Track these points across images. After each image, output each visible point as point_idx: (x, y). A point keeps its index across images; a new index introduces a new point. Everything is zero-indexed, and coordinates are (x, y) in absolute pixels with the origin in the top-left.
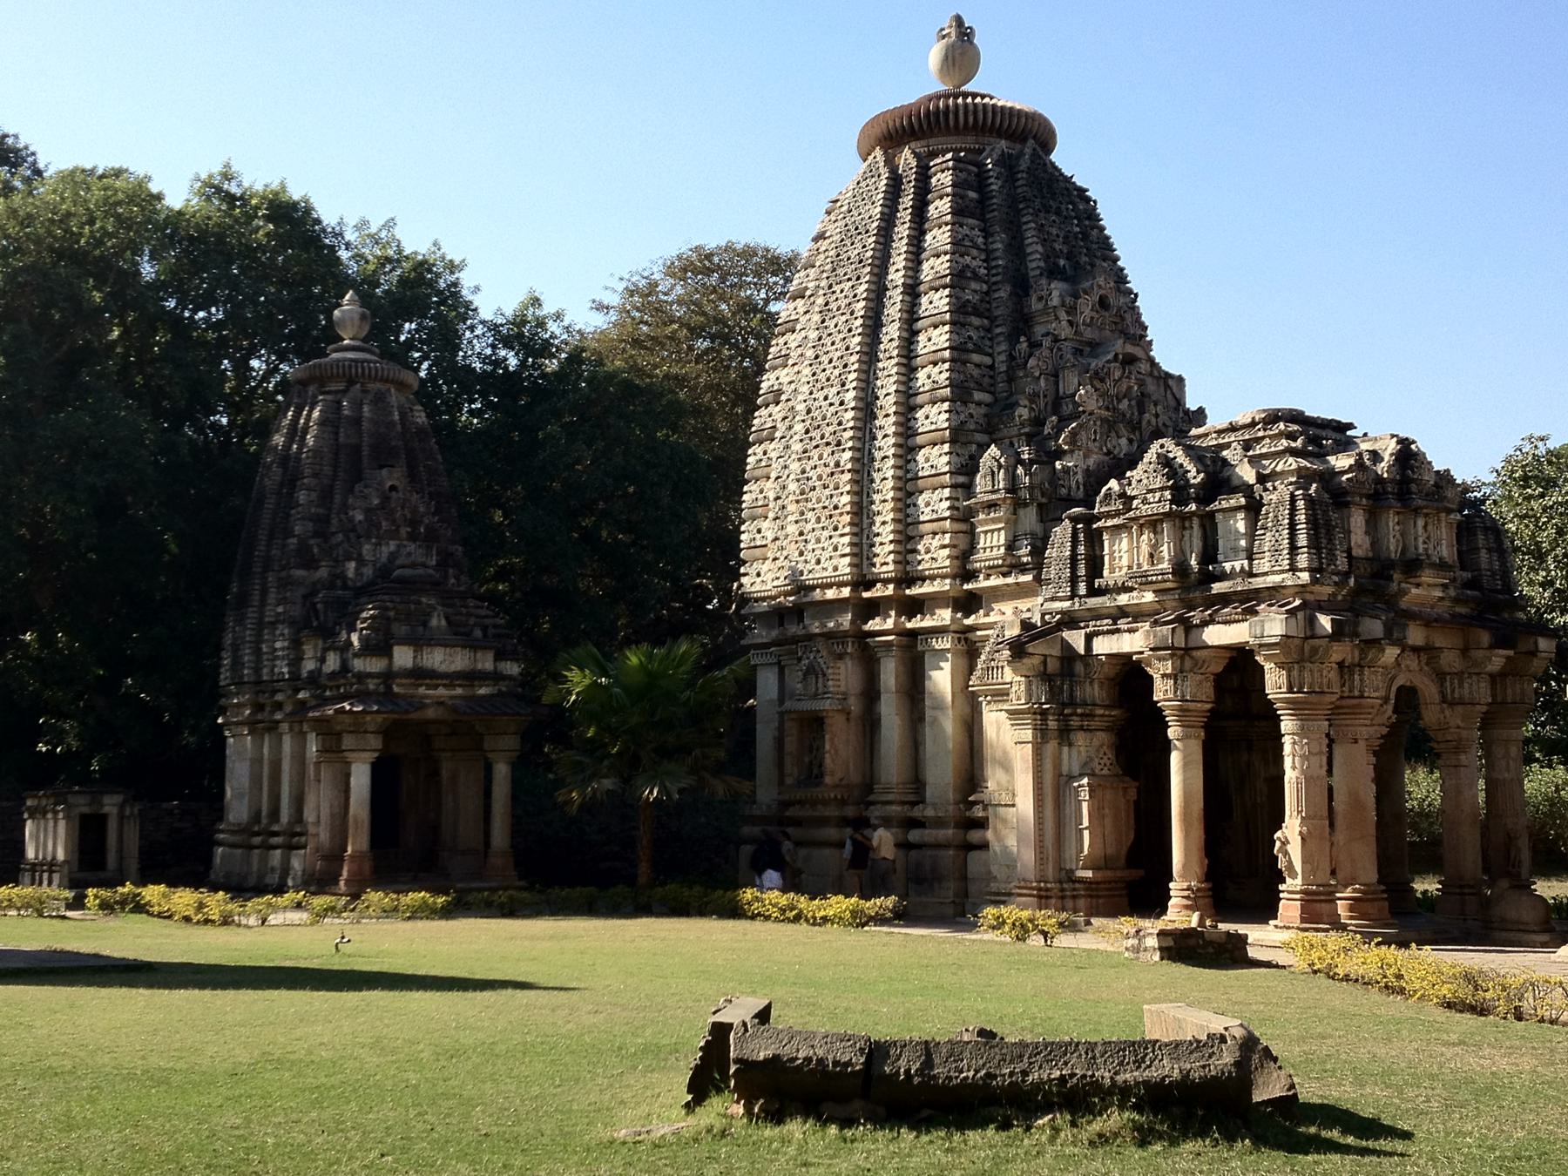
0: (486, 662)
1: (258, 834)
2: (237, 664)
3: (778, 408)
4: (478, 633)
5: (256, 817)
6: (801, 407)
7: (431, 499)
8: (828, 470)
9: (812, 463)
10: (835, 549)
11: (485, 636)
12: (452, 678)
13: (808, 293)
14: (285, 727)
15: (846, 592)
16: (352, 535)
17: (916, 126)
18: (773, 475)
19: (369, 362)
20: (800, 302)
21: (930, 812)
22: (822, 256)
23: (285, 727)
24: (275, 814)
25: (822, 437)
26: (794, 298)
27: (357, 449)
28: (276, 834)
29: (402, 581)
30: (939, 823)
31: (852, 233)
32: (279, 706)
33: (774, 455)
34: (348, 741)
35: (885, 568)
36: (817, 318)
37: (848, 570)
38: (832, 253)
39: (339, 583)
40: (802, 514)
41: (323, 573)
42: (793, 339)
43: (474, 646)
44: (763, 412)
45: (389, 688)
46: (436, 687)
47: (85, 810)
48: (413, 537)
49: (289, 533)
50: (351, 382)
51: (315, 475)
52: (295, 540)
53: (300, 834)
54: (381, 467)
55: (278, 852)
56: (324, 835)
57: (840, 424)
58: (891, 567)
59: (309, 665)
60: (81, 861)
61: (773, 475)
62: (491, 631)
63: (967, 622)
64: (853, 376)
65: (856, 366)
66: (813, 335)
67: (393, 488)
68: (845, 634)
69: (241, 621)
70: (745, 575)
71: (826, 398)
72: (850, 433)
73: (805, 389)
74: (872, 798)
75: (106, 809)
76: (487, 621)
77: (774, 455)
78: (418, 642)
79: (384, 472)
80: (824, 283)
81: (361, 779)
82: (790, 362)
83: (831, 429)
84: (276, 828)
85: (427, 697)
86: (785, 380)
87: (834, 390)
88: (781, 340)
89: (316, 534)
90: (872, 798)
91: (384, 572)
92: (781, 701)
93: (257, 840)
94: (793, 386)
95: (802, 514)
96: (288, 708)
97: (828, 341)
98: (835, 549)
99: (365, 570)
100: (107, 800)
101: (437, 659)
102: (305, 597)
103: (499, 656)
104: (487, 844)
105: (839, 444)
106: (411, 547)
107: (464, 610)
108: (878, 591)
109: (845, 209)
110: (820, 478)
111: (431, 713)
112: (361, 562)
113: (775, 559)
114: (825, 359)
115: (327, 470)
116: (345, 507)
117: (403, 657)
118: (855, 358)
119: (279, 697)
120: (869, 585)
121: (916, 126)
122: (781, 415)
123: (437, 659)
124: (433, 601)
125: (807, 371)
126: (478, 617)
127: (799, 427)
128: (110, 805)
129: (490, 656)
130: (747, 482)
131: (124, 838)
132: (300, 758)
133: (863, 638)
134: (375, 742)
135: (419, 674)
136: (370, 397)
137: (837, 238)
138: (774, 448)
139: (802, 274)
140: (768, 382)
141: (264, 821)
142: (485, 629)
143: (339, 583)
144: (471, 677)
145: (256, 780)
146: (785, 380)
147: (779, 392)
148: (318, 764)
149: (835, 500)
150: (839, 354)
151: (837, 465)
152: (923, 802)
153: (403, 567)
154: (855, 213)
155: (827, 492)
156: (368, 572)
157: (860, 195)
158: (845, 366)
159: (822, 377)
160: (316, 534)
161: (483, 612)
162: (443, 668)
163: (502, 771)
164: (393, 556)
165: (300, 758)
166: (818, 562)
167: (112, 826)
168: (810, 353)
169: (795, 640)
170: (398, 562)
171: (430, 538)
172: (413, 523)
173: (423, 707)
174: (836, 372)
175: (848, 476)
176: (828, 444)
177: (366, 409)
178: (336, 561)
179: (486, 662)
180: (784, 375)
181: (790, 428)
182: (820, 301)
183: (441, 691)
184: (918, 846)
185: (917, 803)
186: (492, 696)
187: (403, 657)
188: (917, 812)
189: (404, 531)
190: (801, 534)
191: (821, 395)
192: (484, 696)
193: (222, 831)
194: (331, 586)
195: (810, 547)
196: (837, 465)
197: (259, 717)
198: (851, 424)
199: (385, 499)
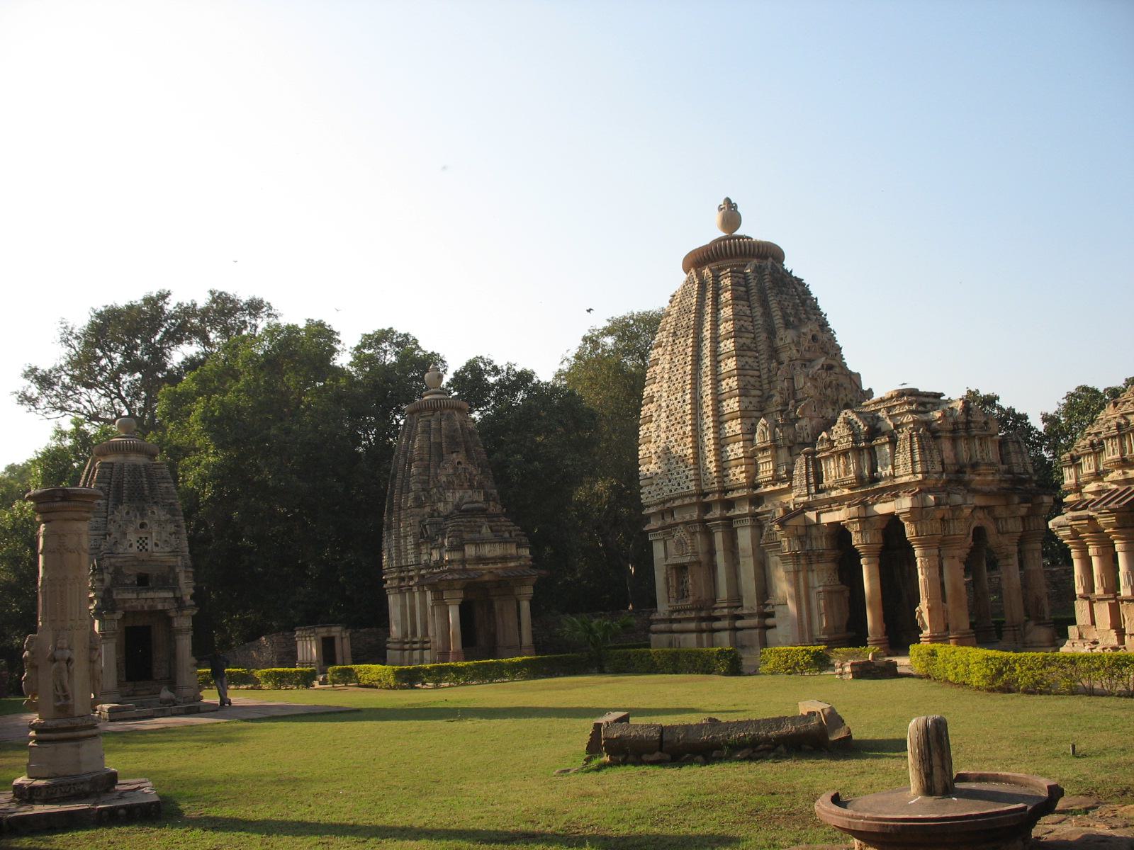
0: (512, 550)
1: (407, 643)
2: (390, 557)
3: (653, 405)
4: (507, 535)
5: (406, 635)
6: (664, 404)
7: (479, 466)
8: (680, 437)
9: (671, 433)
10: (687, 477)
11: (511, 536)
12: (494, 560)
13: (663, 344)
14: (415, 589)
15: (694, 499)
16: (441, 489)
17: (715, 255)
18: (653, 440)
19: (443, 399)
20: (660, 349)
21: (745, 612)
22: (669, 325)
23: (415, 589)
24: (414, 633)
25: (676, 419)
26: (656, 348)
27: (440, 444)
28: (416, 643)
29: (467, 511)
30: (751, 616)
31: (683, 311)
32: (411, 578)
33: (653, 430)
34: (446, 595)
35: (713, 486)
36: (668, 357)
37: (694, 488)
38: (674, 323)
39: (436, 514)
40: (669, 460)
41: (428, 509)
42: (658, 369)
43: (505, 542)
44: (645, 408)
45: (464, 566)
46: (488, 564)
47: (325, 635)
48: (471, 487)
49: (409, 491)
50: (435, 410)
51: (421, 460)
52: (412, 493)
53: (427, 642)
54: (452, 453)
55: (418, 651)
56: (439, 643)
57: (684, 412)
58: (716, 485)
59: (425, 557)
60: (324, 661)
61: (653, 440)
62: (513, 534)
63: (759, 510)
64: (689, 386)
65: (690, 382)
66: (667, 366)
67: (459, 463)
68: (694, 522)
69: (390, 536)
70: (643, 493)
71: (676, 399)
72: (689, 417)
73: (665, 395)
74: (716, 606)
75: (333, 634)
76: (511, 528)
77: (653, 430)
78: (477, 543)
79: (454, 455)
80: (671, 339)
81: (454, 615)
82: (657, 381)
83: (680, 415)
84: (415, 640)
85: (484, 569)
86: (655, 390)
87: (680, 394)
88: (652, 370)
89: (423, 490)
90: (716, 606)
91: (457, 507)
92: (666, 558)
93: (407, 646)
94: (659, 393)
95: (669, 460)
96: (416, 579)
97: (675, 369)
98: (687, 477)
99: (448, 506)
100: (334, 629)
101: (487, 551)
102: (420, 522)
103: (519, 546)
104: (521, 643)
105: (684, 422)
106: (470, 492)
107: (499, 523)
108: (710, 498)
109: (678, 300)
110: (676, 441)
111: (487, 578)
112: (446, 502)
113: (657, 484)
114: (674, 378)
115: (427, 457)
116: (436, 475)
117: (470, 551)
118: (689, 377)
119: (411, 574)
120: (706, 495)
121: (715, 255)
122: (655, 409)
123: (487, 551)
124: (483, 520)
125: (665, 385)
126: (507, 526)
127: (664, 415)
128: (336, 631)
129: (514, 546)
130: (640, 445)
131: (343, 645)
132: (424, 603)
133: (703, 522)
134: (460, 594)
135: (480, 559)
136: (445, 417)
137: (675, 315)
138: (652, 426)
139: (660, 334)
140: (647, 392)
141: (410, 636)
142: (510, 533)
143: (436, 514)
144: (504, 559)
145: (403, 614)
146: (655, 390)
147: (653, 397)
148: (432, 607)
149: (685, 452)
150: (680, 376)
151: (684, 433)
152: (742, 606)
153: (466, 503)
154: (683, 302)
155: (681, 448)
156: (450, 507)
157: (685, 292)
158: (684, 382)
159: (673, 388)
160: (423, 490)
161: (508, 524)
162: (490, 555)
163: (525, 605)
164: (461, 498)
165: (424, 603)
166: (679, 484)
167: (337, 641)
168: (666, 376)
169: (670, 526)
170: (464, 501)
171: (481, 486)
172: (470, 481)
173: (483, 575)
174: (680, 385)
175: (690, 439)
176: (679, 423)
177: (443, 423)
178: (434, 502)
179: (512, 550)
180: (655, 387)
181: (659, 416)
182: (669, 348)
183: (490, 566)
184: (741, 629)
185: (738, 607)
186: (517, 566)
187: (470, 551)
188: (738, 612)
189: (466, 485)
190: (669, 470)
191: (673, 398)
192: (511, 567)
193: (389, 642)
194: (432, 516)
195: (674, 477)
196: (684, 433)
197: (403, 584)
198: (690, 412)
199: (455, 469)
